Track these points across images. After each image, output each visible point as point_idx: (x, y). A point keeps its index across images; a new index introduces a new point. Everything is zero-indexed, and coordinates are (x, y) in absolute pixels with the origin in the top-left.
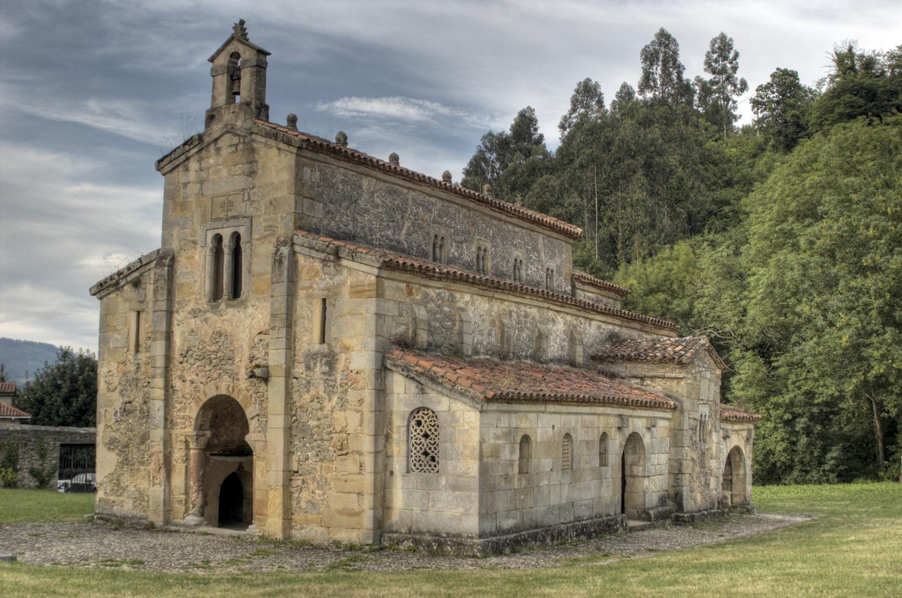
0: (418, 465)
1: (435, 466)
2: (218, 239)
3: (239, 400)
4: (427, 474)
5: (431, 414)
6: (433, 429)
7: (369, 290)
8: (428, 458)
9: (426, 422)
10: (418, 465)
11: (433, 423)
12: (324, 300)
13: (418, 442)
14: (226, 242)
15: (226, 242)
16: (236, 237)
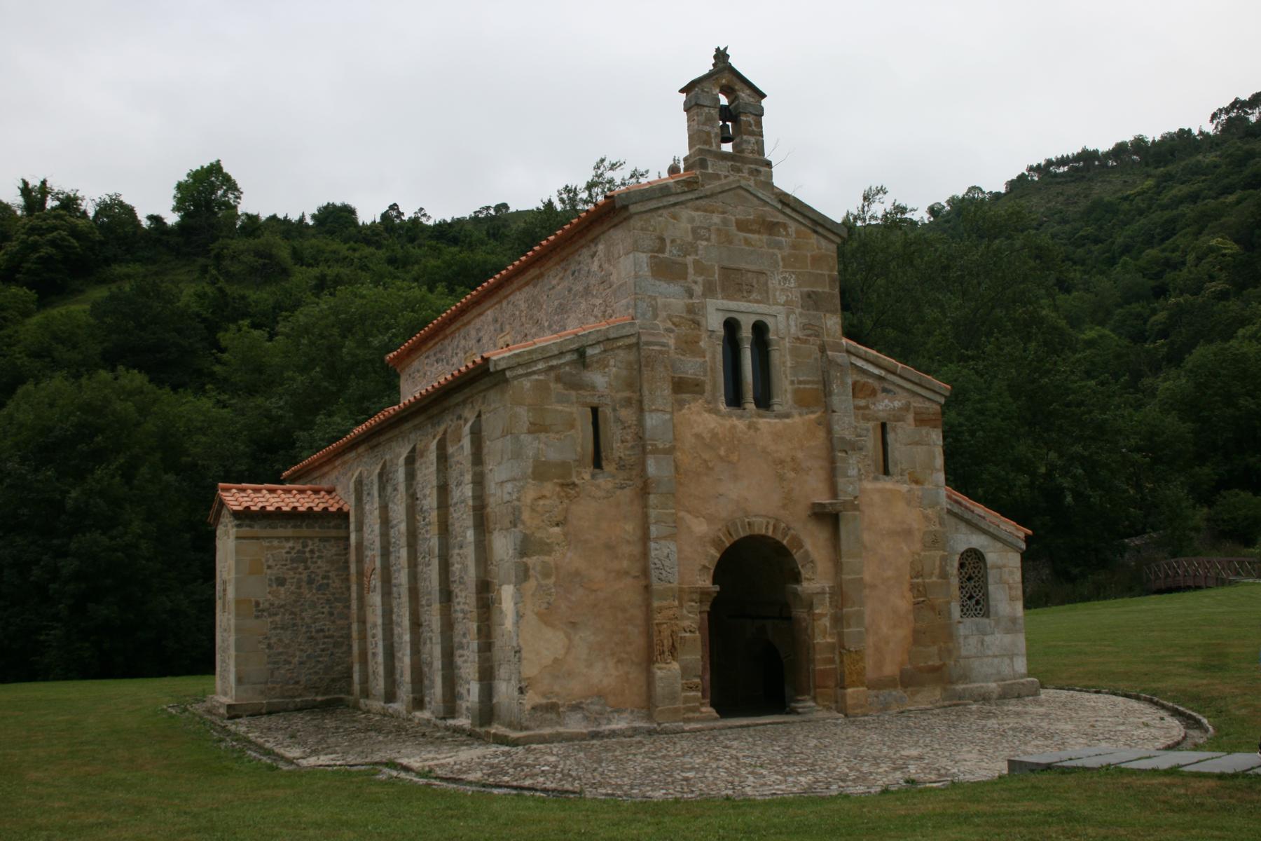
0: (965, 610)
1: (981, 610)
2: (731, 326)
3: (785, 542)
4: (977, 619)
5: (974, 555)
6: (976, 572)
7: (935, 420)
8: (974, 601)
9: (970, 563)
10: (965, 610)
11: (976, 565)
12: (884, 426)
13: (964, 585)
14: (746, 333)
15: (746, 333)
16: (760, 329)
